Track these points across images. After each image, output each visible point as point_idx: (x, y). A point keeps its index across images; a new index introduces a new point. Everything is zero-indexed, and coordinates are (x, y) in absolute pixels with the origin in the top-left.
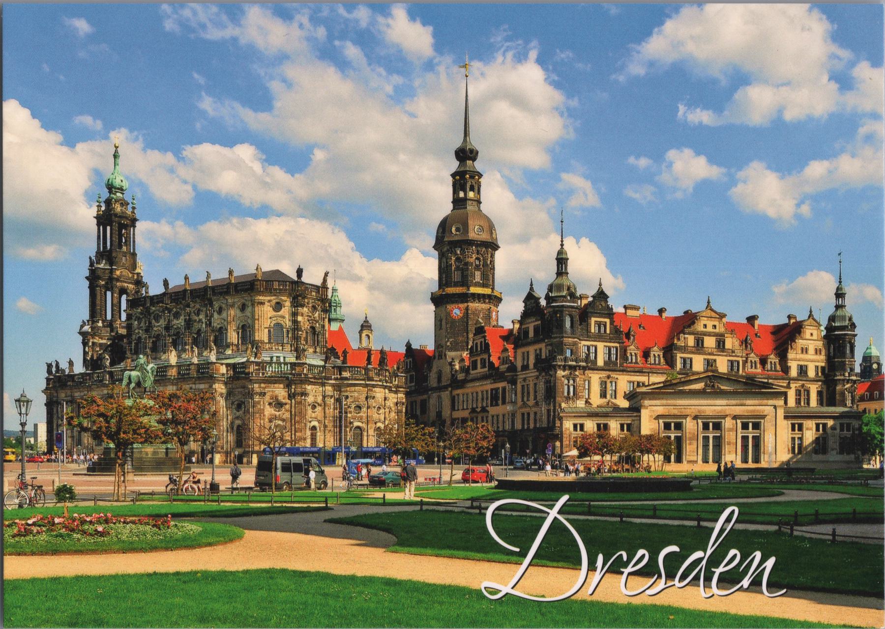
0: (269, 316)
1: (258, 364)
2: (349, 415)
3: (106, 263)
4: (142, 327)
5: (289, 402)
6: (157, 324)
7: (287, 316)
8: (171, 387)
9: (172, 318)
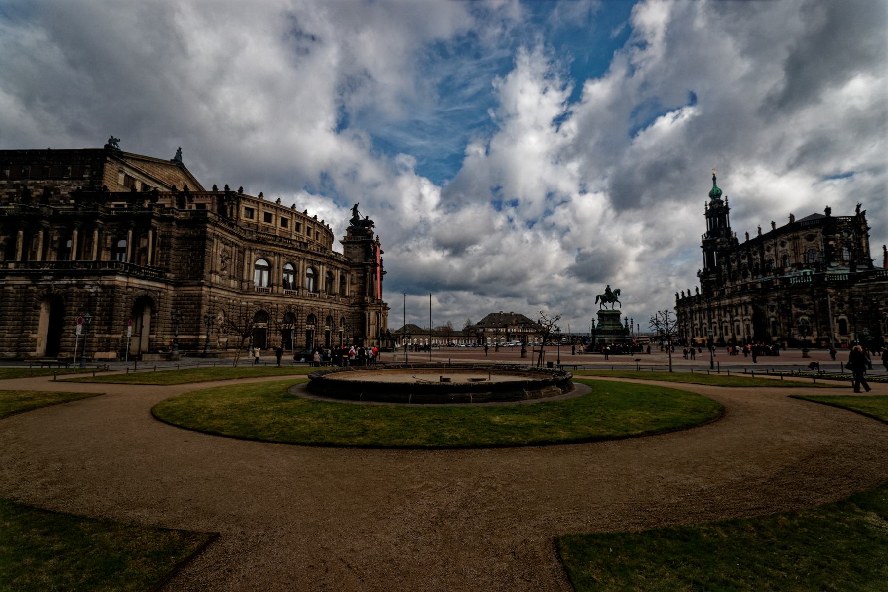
1: (780, 279)
6: (733, 265)
7: (820, 243)
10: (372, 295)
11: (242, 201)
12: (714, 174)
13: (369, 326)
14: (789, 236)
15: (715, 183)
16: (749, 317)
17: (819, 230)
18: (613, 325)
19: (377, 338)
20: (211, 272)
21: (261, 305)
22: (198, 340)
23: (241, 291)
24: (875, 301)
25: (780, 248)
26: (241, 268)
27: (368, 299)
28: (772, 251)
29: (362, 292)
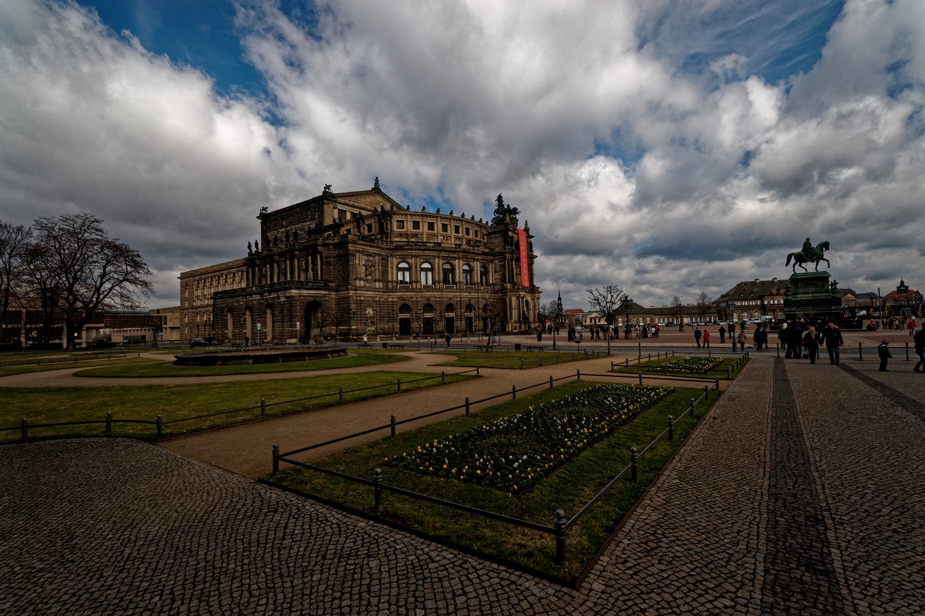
10: (512, 281)
11: (394, 216)
13: (511, 310)
18: (813, 293)
19: (519, 322)
20: (355, 279)
21: (404, 300)
22: (351, 330)
23: (387, 290)
26: (385, 272)
27: (509, 286)
29: (503, 280)
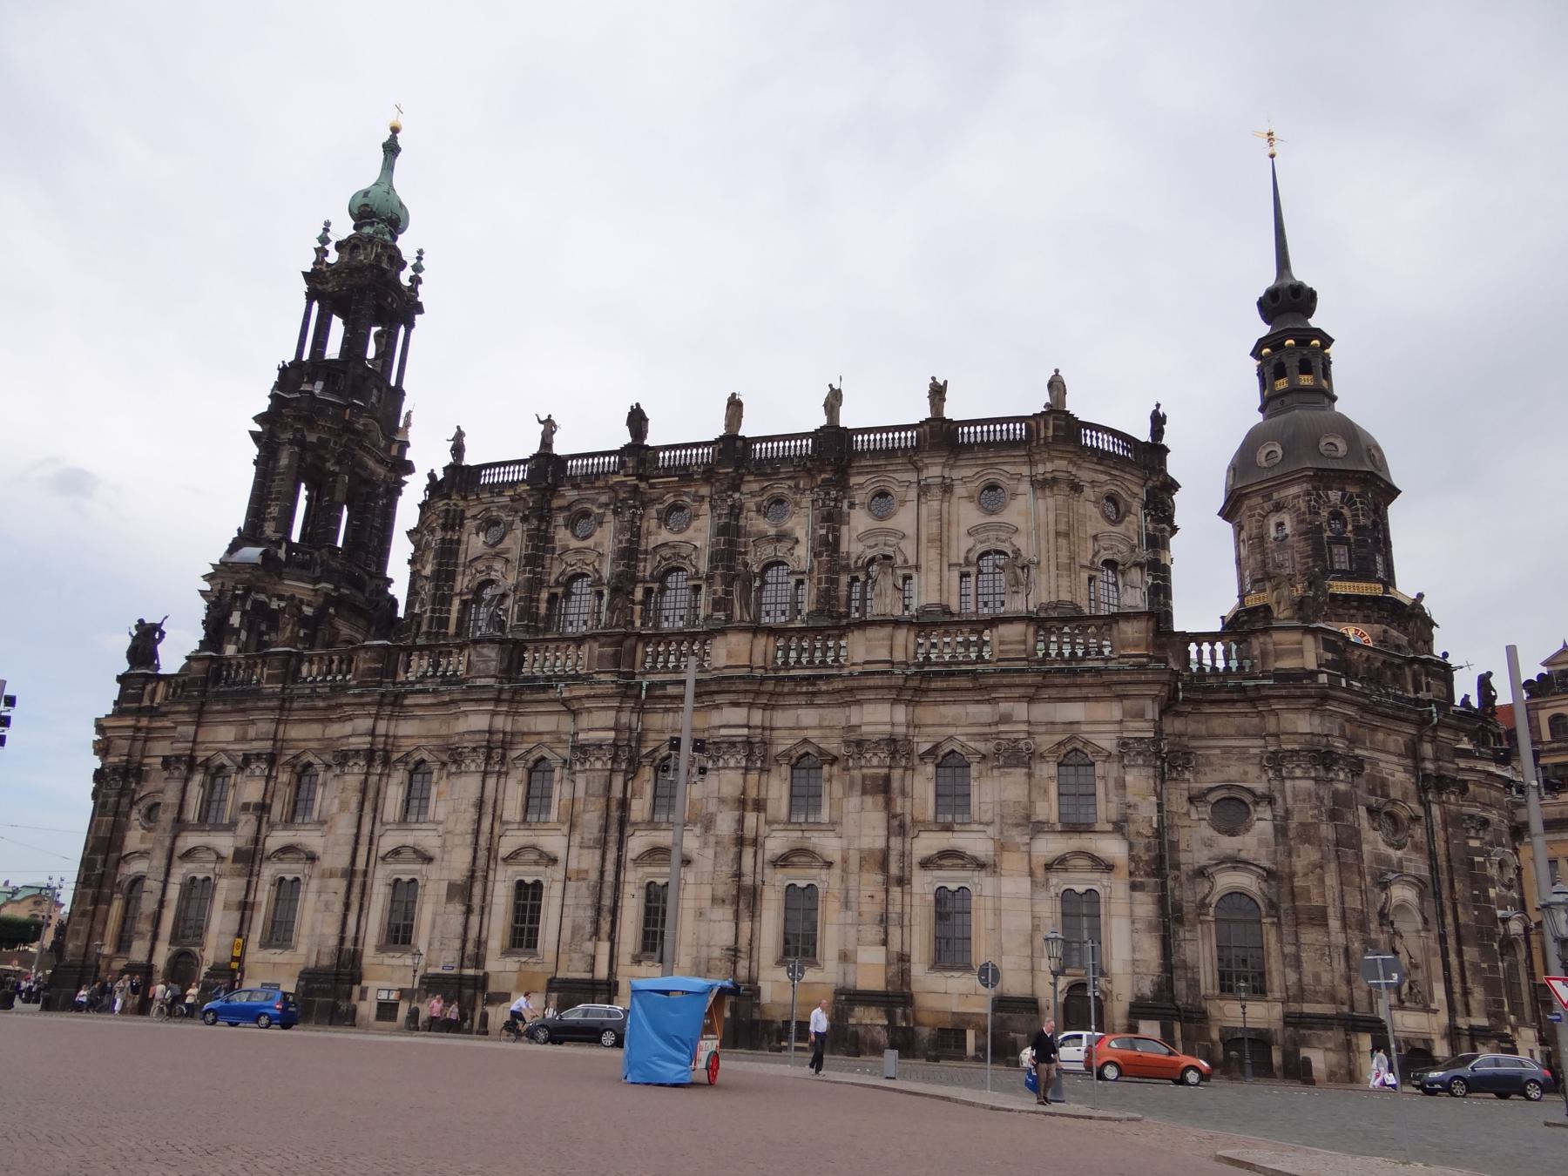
0: (1094, 533)
2: (1492, 893)
3: (324, 390)
4: (507, 550)
5: (1420, 811)
8: (887, 706)
9: (653, 523)
12: (395, 130)
14: (1040, 469)
15: (388, 166)
16: (1112, 848)
17: (1136, 489)
24: (1479, 852)
25: (967, 514)
28: (904, 519)
